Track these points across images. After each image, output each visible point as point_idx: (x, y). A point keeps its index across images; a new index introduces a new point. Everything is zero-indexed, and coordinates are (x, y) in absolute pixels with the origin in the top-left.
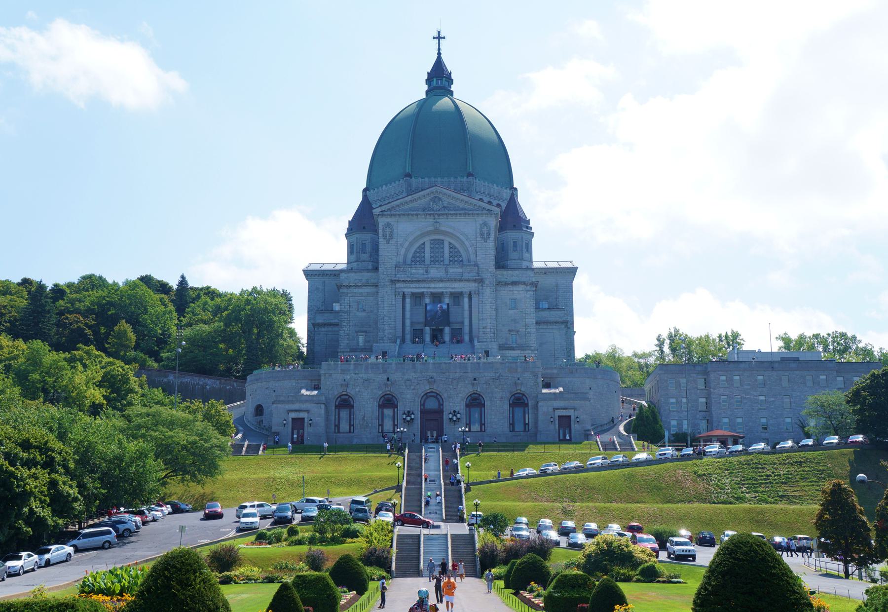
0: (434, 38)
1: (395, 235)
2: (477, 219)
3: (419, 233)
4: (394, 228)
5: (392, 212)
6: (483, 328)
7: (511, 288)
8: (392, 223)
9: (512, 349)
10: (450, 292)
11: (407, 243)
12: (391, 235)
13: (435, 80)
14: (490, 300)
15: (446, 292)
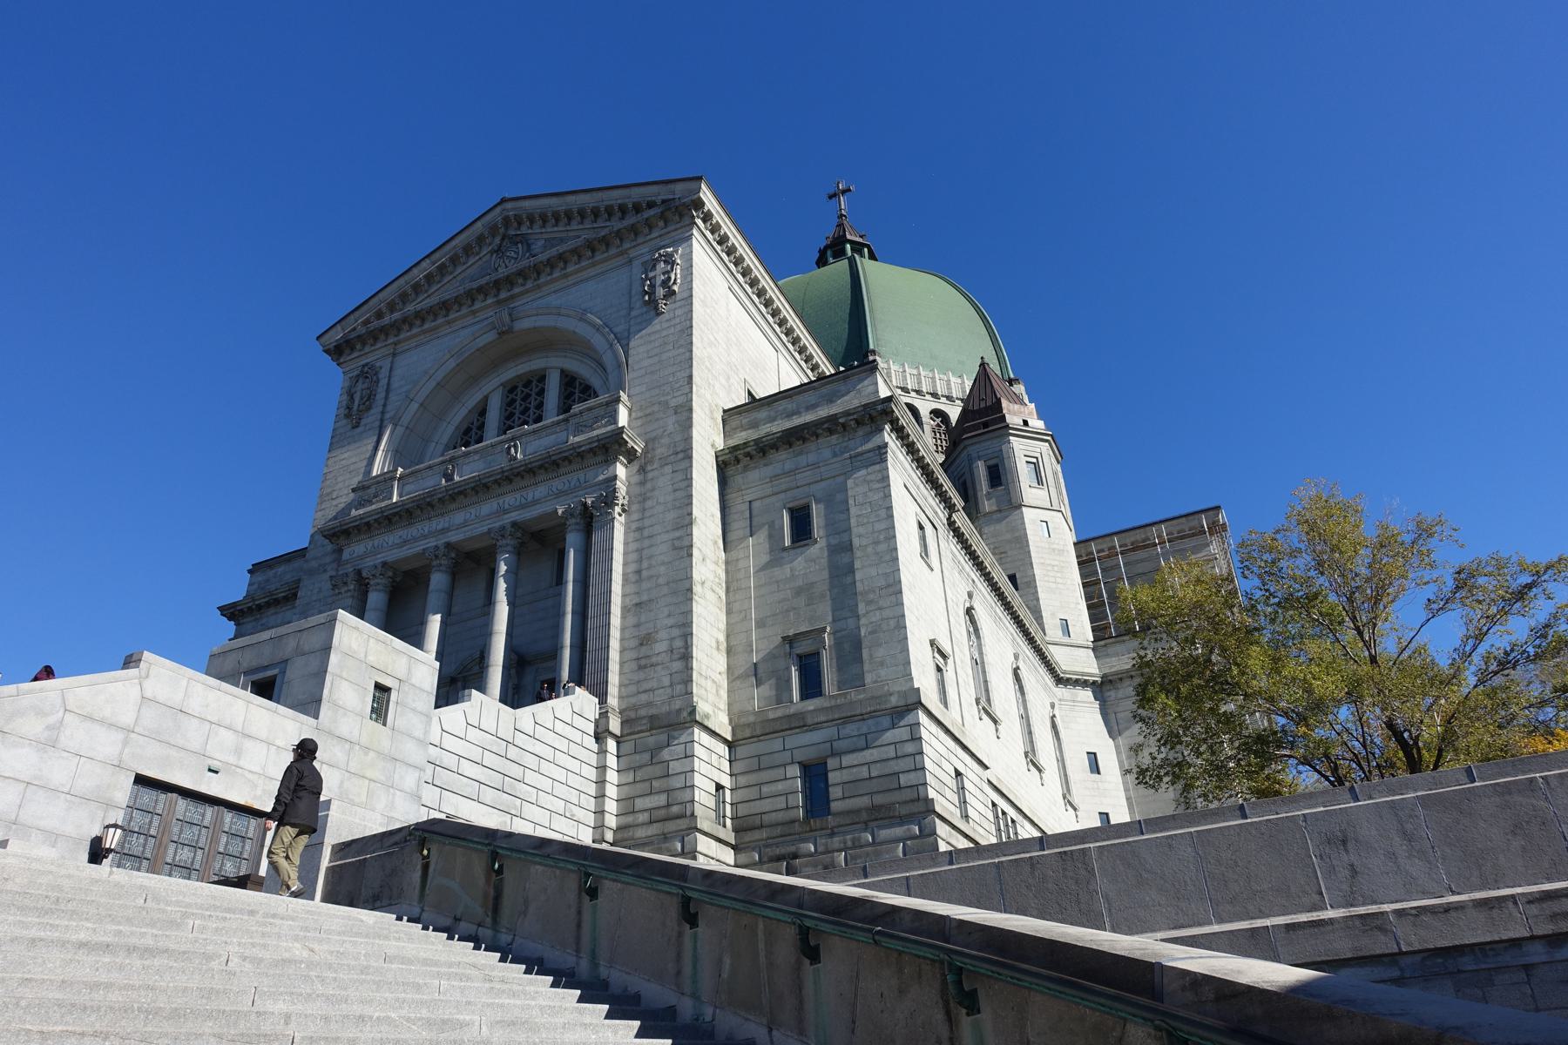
0: (831, 197)
1: (380, 395)
2: (633, 253)
3: (452, 364)
4: (383, 374)
5: (376, 324)
6: (641, 644)
7: (782, 460)
8: (378, 365)
9: (798, 723)
10: (514, 524)
11: (415, 406)
12: (369, 398)
13: (829, 253)
14: (671, 515)
15: (503, 528)
